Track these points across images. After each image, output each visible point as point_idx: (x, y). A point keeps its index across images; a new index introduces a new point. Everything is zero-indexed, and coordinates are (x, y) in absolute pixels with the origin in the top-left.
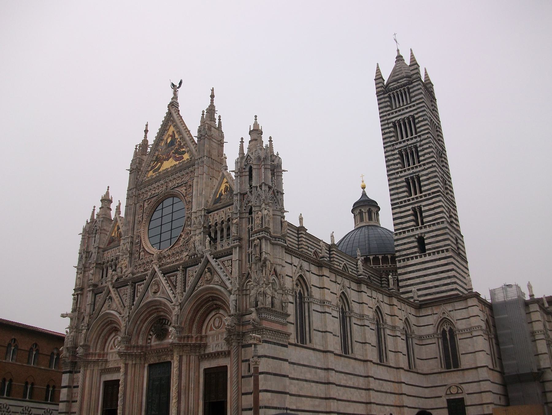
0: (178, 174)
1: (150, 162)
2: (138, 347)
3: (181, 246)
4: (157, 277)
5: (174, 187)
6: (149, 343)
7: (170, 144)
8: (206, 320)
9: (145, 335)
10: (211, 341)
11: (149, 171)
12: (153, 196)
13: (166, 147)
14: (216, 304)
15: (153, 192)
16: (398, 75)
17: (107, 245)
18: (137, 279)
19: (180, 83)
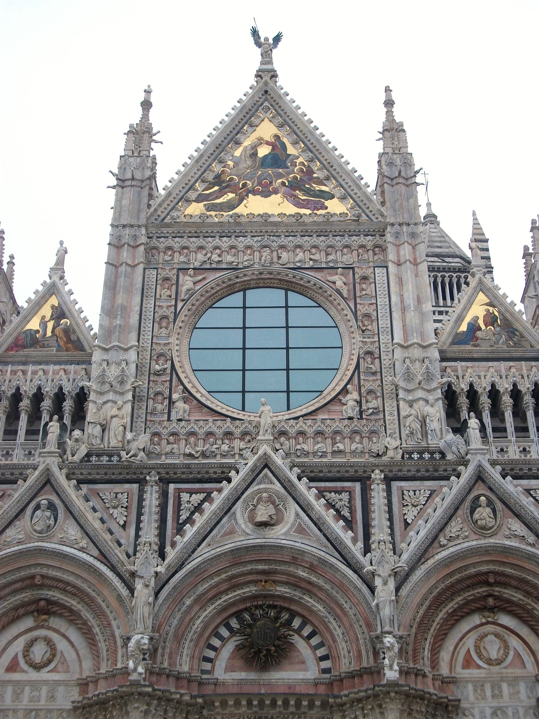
0: (315, 240)
1: (193, 180)
2: (178, 678)
3: (350, 418)
4: (272, 483)
5: (298, 264)
6: (203, 672)
7: (269, 161)
8: (449, 636)
9: (196, 645)
10: (472, 698)
11: (189, 201)
12: (214, 266)
13: (255, 161)
14: (496, 598)
15: (215, 258)
16: (441, 247)
17: (7, 350)
18: (183, 473)
19: (277, 39)
